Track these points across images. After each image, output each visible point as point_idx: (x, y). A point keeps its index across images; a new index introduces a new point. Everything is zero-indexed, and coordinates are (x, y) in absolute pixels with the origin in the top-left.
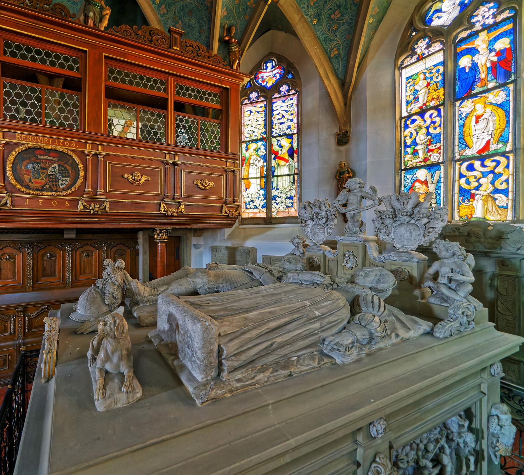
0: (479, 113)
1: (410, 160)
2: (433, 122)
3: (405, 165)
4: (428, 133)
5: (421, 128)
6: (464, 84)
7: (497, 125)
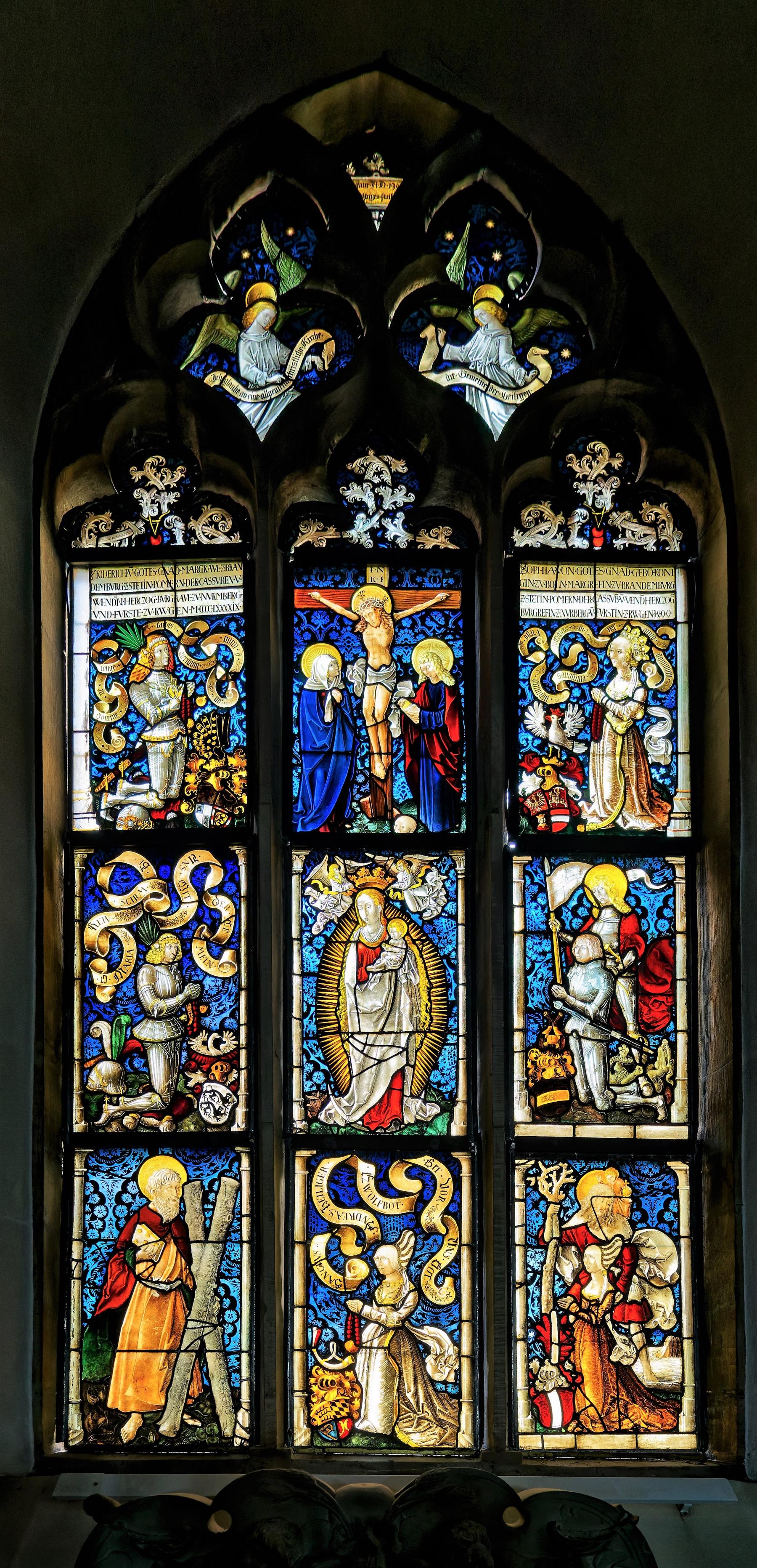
0: (369, 933)
1: (111, 1089)
2: (207, 917)
3: (87, 1115)
4: (185, 968)
5: (159, 928)
6: (319, 773)
7: (424, 1013)
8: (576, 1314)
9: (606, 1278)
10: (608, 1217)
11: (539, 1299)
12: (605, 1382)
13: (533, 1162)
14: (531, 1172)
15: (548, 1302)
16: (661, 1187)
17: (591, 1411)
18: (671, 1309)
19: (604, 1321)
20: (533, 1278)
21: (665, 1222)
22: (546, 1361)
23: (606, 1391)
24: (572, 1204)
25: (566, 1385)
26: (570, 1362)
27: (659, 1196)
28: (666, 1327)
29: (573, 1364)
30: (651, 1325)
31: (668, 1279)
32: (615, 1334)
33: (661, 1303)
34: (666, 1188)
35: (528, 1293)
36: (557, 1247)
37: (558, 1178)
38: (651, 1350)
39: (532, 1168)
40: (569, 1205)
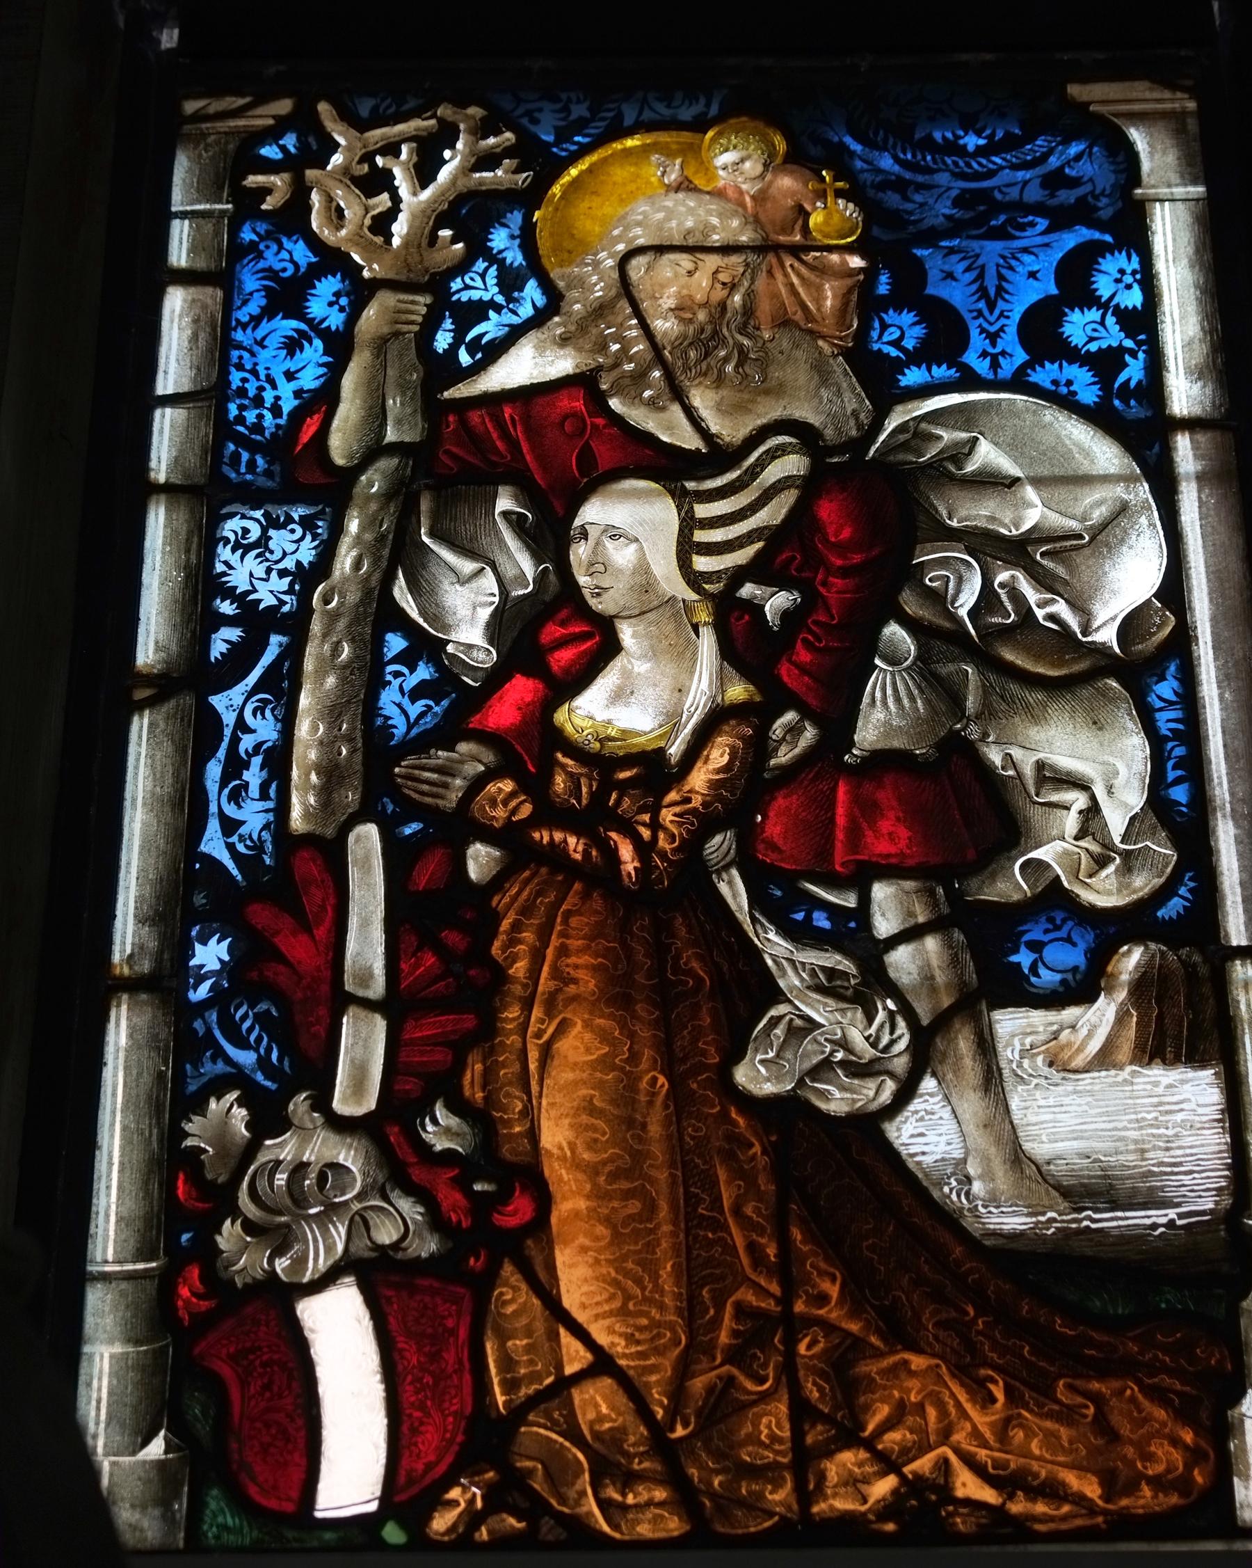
8: (508, 837)
9: (707, 643)
10: (718, 343)
11: (278, 759)
12: (698, 1218)
13: (284, 106)
14: (270, 152)
15: (331, 774)
16: (1034, 194)
17: (597, 1404)
18: (1135, 799)
19: (693, 874)
20: (240, 659)
21: (1072, 354)
22: (299, 1104)
23: (704, 1273)
24: (510, 283)
25: (427, 1246)
26: (458, 1106)
27: (1031, 237)
28: (1104, 892)
29: (480, 1119)
30: (1012, 884)
31: (1107, 635)
32: (774, 944)
33: (1066, 762)
34: (1067, 196)
35: (202, 733)
36: (401, 497)
37: (424, 173)
38: (1013, 1026)
39: (273, 134)
40: (492, 292)
